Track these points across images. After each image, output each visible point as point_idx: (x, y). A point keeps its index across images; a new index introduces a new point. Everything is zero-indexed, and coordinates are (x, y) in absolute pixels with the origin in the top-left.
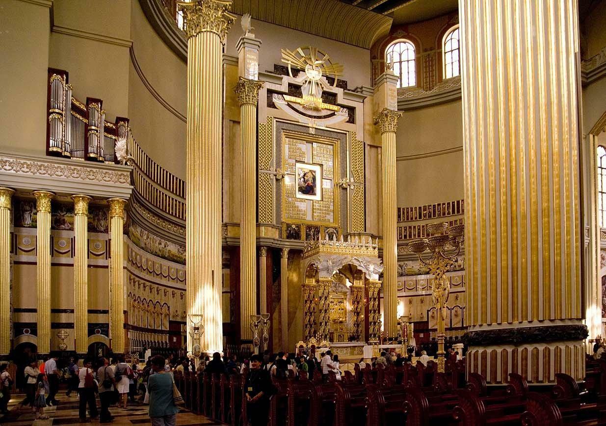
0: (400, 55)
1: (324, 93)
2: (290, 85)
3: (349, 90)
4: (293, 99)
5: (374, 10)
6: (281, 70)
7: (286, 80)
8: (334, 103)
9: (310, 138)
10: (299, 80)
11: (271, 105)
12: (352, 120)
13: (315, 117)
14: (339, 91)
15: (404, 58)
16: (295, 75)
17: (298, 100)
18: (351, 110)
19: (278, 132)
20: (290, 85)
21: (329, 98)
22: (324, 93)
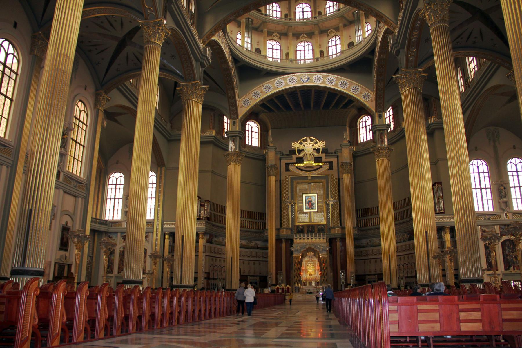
0: (366, 122)
1: (315, 158)
2: (296, 158)
3: (329, 153)
4: (299, 165)
5: (342, 108)
6: (293, 152)
7: (294, 156)
8: (321, 162)
9: (310, 181)
10: (301, 155)
11: (287, 170)
12: (331, 168)
13: (311, 171)
14: (323, 156)
15: (367, 124)
16: (299, 153)
17: (302, 165)
18: (331, 163)
19: (292, 182)
20: (296, 158)
21: (318, 160)
22: (315, 158)
